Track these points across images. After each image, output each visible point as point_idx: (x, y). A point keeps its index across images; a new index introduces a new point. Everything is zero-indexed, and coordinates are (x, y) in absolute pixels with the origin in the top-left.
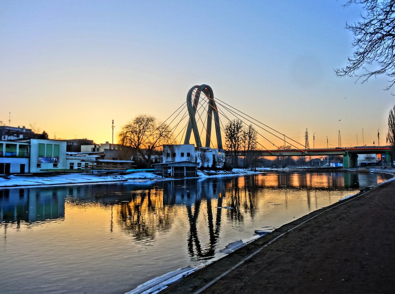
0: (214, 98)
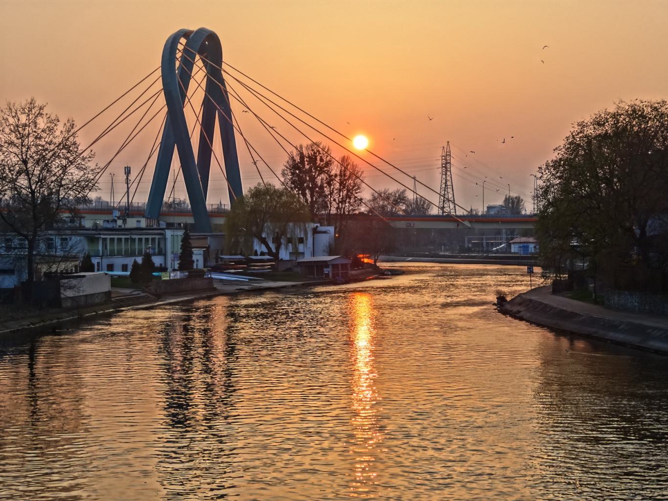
0: (224, 66)
